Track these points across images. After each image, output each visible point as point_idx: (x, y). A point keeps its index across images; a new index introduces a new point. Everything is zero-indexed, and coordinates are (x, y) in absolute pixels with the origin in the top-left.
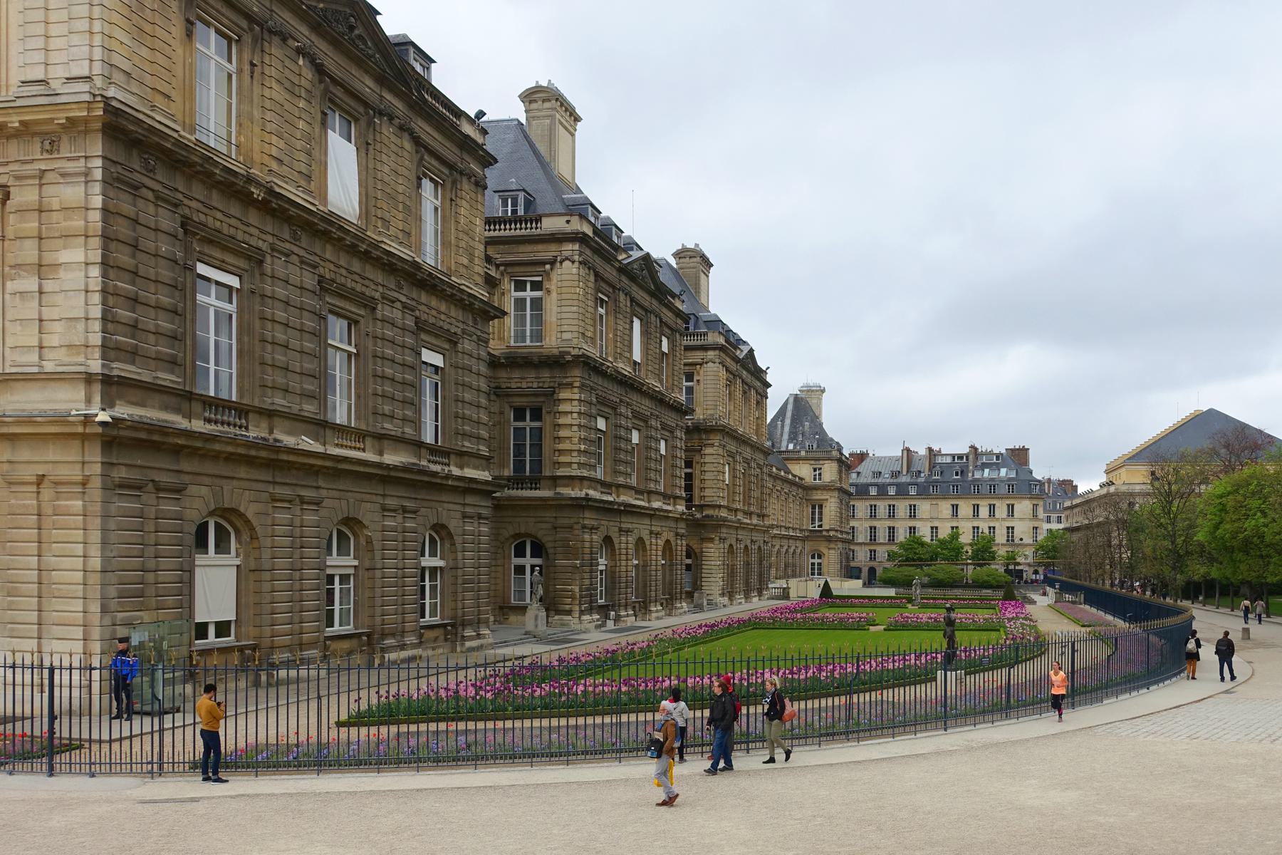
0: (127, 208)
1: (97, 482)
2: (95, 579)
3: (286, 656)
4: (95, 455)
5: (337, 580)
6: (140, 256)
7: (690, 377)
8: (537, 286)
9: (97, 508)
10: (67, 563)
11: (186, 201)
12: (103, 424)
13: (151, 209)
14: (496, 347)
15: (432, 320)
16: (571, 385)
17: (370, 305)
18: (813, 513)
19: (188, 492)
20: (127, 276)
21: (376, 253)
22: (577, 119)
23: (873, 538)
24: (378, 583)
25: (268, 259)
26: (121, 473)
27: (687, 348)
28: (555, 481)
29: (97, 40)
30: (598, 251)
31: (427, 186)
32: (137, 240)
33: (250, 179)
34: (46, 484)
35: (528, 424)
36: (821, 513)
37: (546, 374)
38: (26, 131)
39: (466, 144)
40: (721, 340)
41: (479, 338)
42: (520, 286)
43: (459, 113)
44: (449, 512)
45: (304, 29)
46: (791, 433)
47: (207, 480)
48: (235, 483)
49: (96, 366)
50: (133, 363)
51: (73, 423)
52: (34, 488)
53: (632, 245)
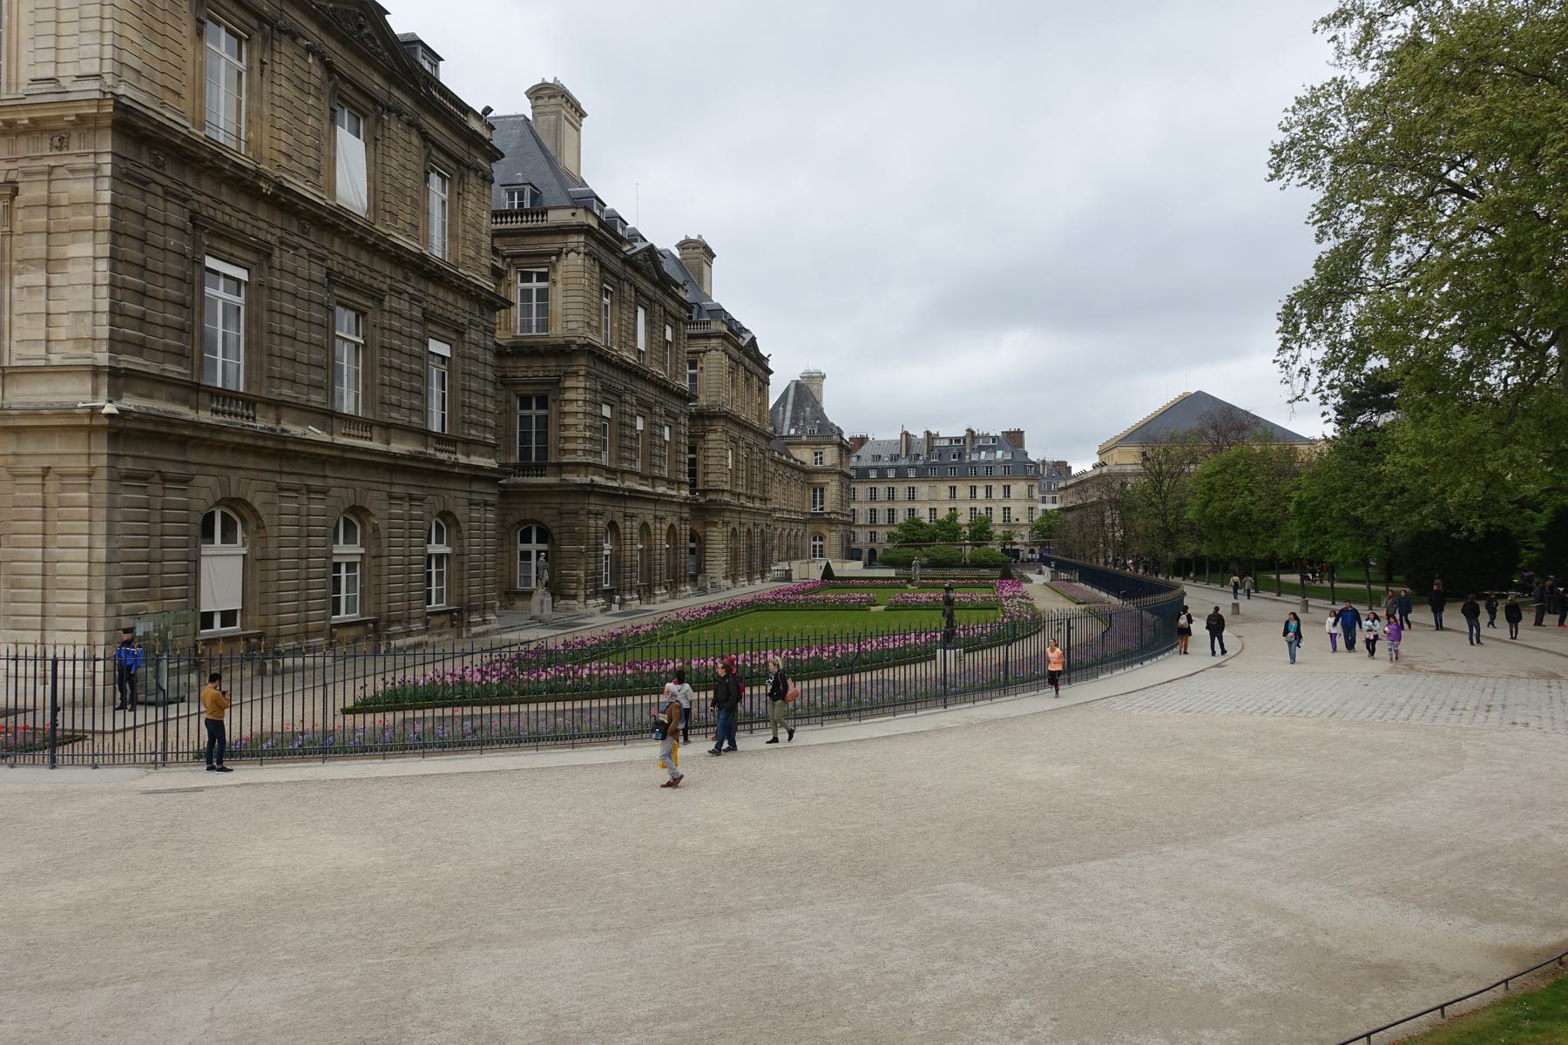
0: (136, 203)
3: (292, 644)
5: (343, 568)
6: (148, 249)
7: (693, 365)
8: (542, 277)
13: (160, 204)
14: (502, 337)
15: (439, 311)
16: (576, 374)
17: (377, 296)
19: (194, 482)
21: (384, 246)
22: (583, 115)
24: (385, 570)
25: (277, 252)
27: (691, 337)
28: (560, 467)
30: (603, 242)
31: (435, 180)
32: (145, 234)
33: (259, 175)
35: (534, 412)
36: (822, 496)
37: (552, 363)
38: (36, 128)
39: (474, 140)
40: (724, 329)
41: (486, 328)
42: (526, 277)
43: (467, 110)
44: (456, 499)
45: (314, 29)
46: (792, 418)
47: (214, 471)
48: (242, 473)
52: (39, 481)
53: (636, 236)
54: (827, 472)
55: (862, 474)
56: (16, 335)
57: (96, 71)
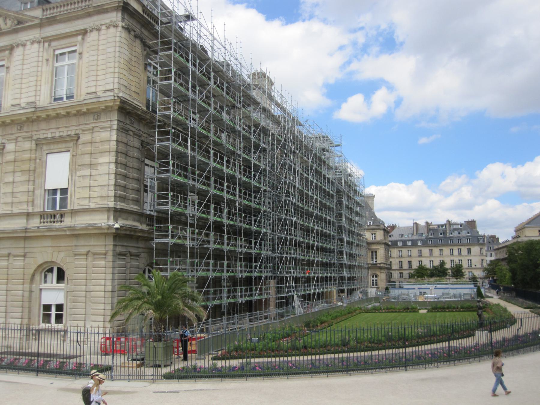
1: (111, 253)
2: (109, 295)
4: (110, 242)
6: (128, 158)
9: (111, 264)
10: (98, 288)
11: (143, 135)
12: (117, 229)
18: (372, 255)
20: (123, 167)
23: (401, 267)
26: (119, 249)
29: (117, 75)
32: (127, 152)
34: (90, 254)
36: (376, 255)
49: (111, 204)
50: (124, 202)
51: (104, 229)
54: (378, 243)
55: (395, 244)
56: (77, 196)
57: (111, 88)
